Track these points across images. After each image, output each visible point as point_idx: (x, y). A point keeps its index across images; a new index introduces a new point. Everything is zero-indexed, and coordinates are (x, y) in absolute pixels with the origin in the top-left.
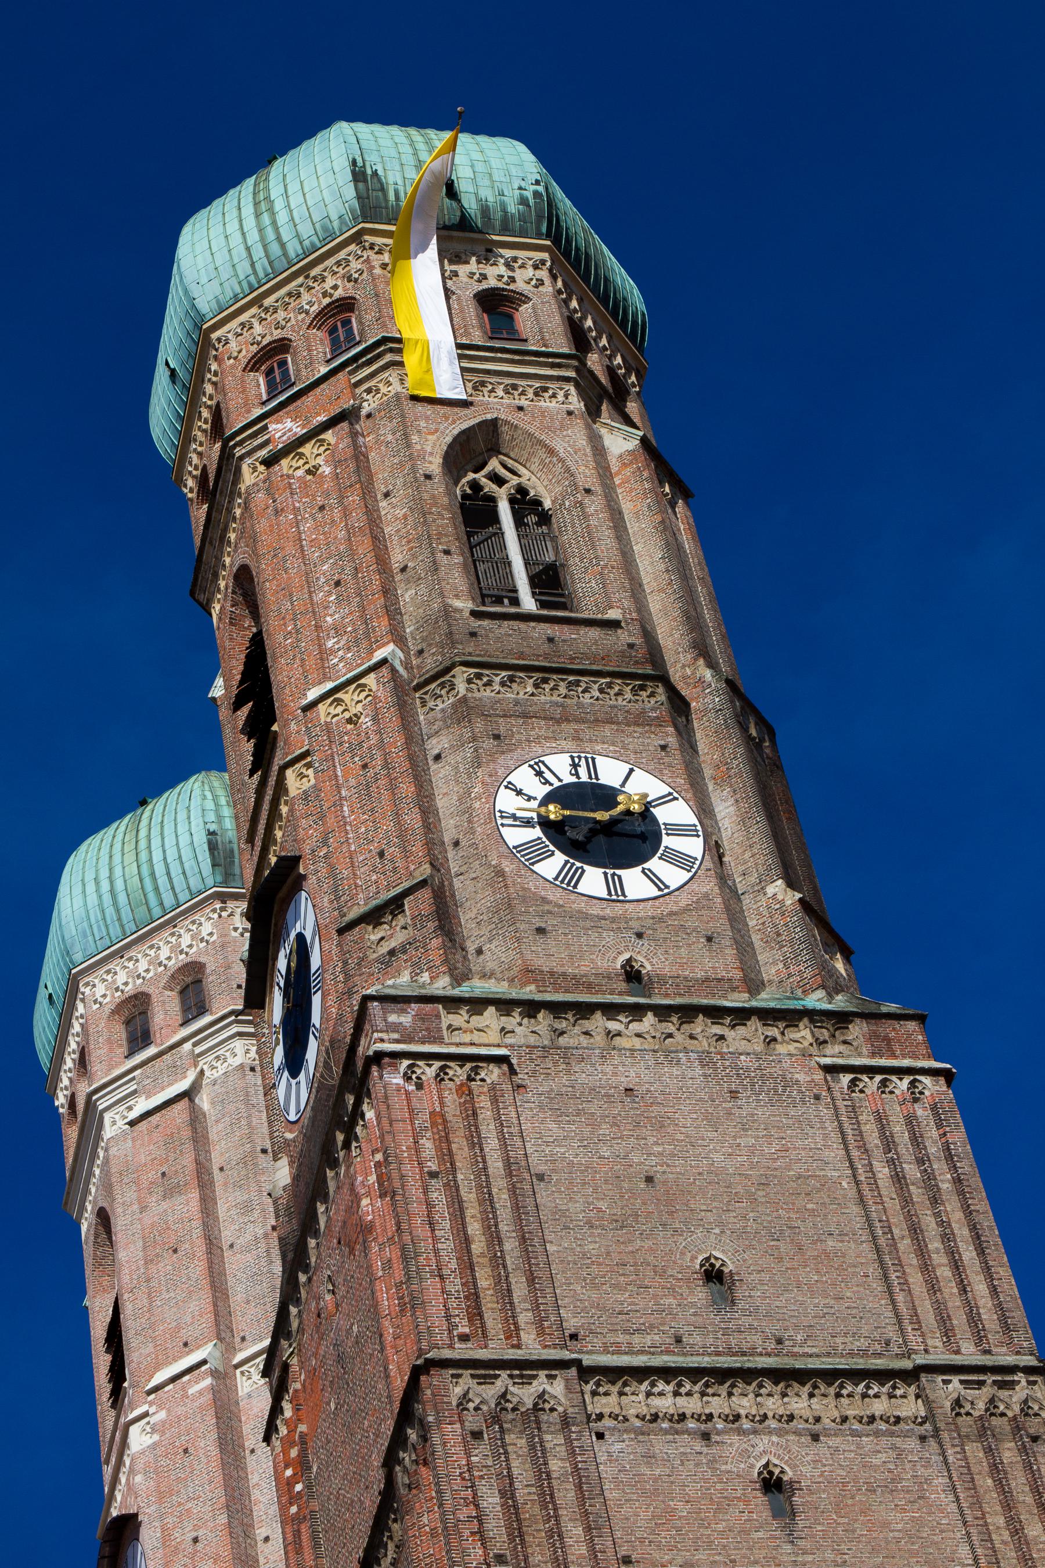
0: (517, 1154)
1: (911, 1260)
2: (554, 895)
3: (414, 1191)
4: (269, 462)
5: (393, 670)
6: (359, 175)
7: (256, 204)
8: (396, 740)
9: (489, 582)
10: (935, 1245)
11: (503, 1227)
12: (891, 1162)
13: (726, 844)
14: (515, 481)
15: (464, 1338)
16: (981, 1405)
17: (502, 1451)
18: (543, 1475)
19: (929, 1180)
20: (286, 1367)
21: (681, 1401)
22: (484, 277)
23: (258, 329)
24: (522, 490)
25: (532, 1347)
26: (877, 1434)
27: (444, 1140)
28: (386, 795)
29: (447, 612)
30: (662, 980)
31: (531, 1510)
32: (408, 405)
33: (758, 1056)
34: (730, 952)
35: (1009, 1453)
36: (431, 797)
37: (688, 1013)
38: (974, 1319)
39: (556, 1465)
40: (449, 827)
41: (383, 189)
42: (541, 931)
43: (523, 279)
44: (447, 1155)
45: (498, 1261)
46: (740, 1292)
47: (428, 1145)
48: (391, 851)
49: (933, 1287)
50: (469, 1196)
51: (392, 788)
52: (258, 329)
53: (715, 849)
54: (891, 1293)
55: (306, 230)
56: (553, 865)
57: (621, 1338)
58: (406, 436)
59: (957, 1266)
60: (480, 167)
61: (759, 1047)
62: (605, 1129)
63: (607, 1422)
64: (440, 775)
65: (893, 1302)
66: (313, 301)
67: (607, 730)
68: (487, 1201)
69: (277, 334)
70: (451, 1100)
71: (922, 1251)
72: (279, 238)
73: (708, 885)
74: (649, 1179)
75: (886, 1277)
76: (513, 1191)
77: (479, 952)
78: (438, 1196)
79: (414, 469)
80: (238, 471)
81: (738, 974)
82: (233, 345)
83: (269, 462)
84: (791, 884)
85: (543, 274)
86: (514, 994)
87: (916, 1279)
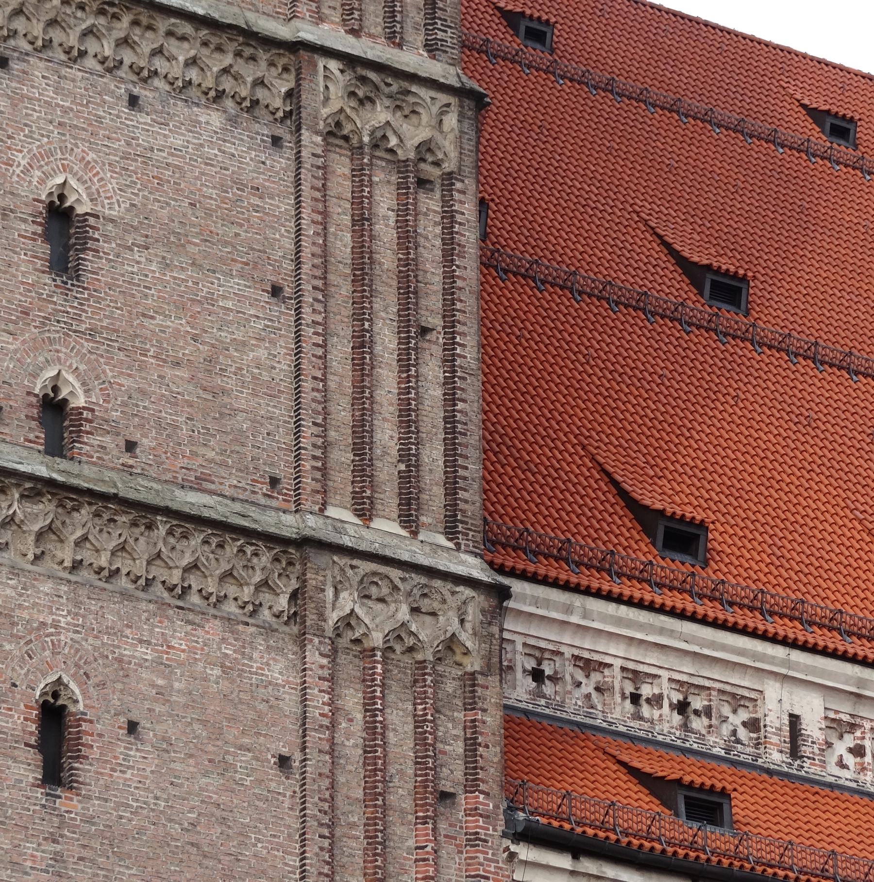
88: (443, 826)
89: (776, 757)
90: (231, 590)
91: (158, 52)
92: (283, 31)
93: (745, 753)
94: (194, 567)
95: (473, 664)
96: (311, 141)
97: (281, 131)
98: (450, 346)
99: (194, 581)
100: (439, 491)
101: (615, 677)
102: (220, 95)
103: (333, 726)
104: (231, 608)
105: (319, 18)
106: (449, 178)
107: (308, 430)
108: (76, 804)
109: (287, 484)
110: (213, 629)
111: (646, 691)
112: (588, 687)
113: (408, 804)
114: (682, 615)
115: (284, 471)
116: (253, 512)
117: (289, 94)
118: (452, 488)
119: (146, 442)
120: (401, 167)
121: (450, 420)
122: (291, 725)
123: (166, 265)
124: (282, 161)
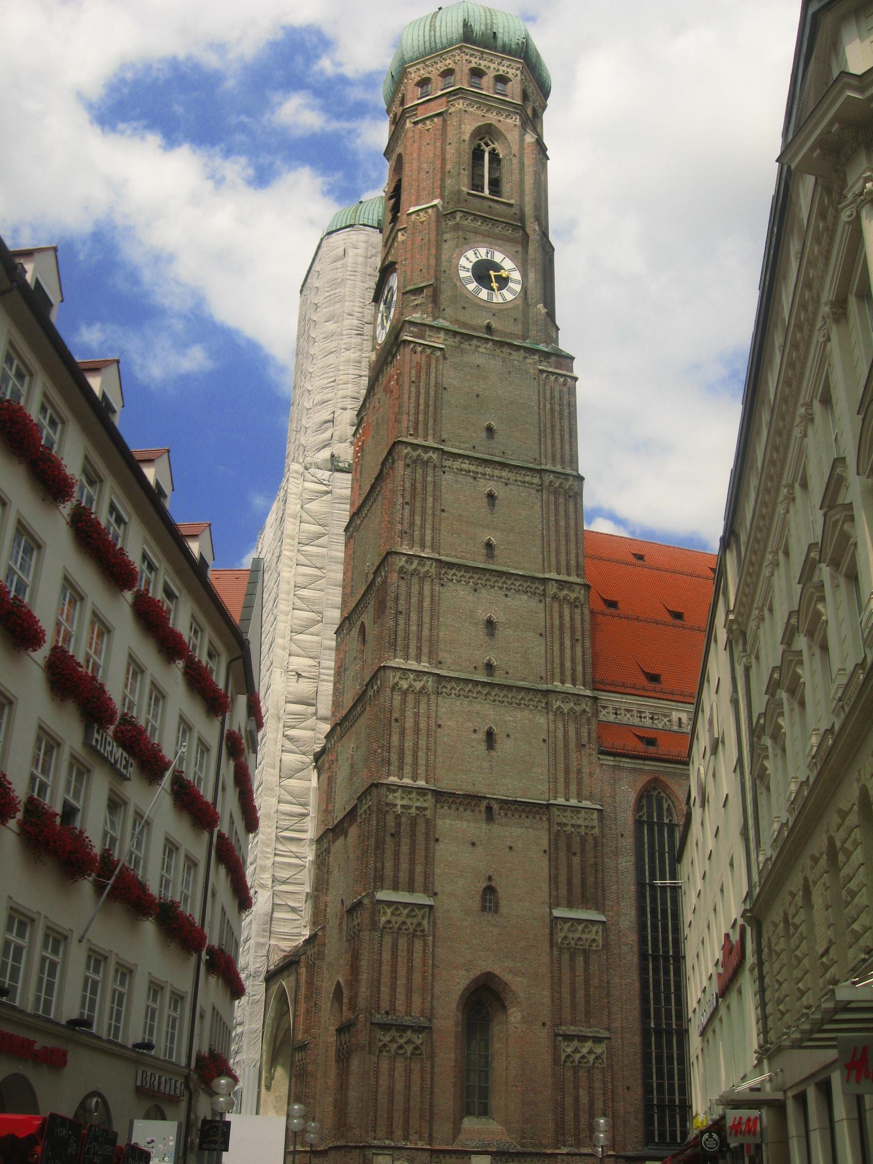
0: (439, 380)
1: (549, 435)
2: (469, 296)
3: (406, 386)
4: (416, 123)
5: (438, 209)
6: (466, 25)
7: (431, 26)
8: (433, 236)
9: (477, 182)
10: (557, 432)
11: (430, 403)
12: (551, 404)
13: (529, 286)
14: (492, 146)
15: (411, 435)
16: (557, 484)
17: (414, 472)
18: (425, 480)
19: (561, 412)
20: (362, 418)
21: (471, 466)
22: (498, 70)
23: (422, 72)
24: (494, 150)
25: (430, 443)
26: (525, 487)
27: (419, 372)
28: (426, 251)
29: (459, 191)
30: (497, 331)
31: (419, 490)
32: (463, 113)
33: (520, 362)
34: (520, 326)
35: (561, 500)
36: (440, 255)
37: (502, 344)
38: (562, 457)
39: (429, 479)
40: (444, 265)
41: (472, 32)
42: (464, 308)
43: (511, 73)
44: (418, 377)
45: (426, 413)
46: (496, 436)
47: (413, 372)
48: (424, 270)
49: (553, 445)
50: (422, 391)
51: (429, 250)
52: (422, 72)
53: (525, 290)
54: (540, 444)
55: (444, 41)
56: (472, 286)
57: (457, 443)
58: (460, 124)
59: (562, 440)
60: (506, 29)
61: (521, 359)
62: (468, 377)
63: (447, 469)
64: (446, 246)
65: (540, 448)
66: (441, 67)
67: (500, 242)
68: (427, 394)
69: (428, 75)
70: (424, 358)
71: (553, 433)
72: (435, 41)
73: (519, 302)
74: (478, 396)
75: (540, 440)
76: (436, 392)
77: (444, 310)
78: (413, 389)
79: (460, 137)
80: (405, 121)
81: (520, 333)
82: (413, 75)
83: (416, 123)
84: (545, 306)
85: (518, 72)
86: (450, 328)
87: (549, 442)
88: (583, 752)
89: (675, 728)
90: (531, 703)
91: (512, 584)
92: (541, 576)
93: (667, 728)
94: (522, 698)
95: (589, 715)
96: (548, 600)
97: (542, 598)
98: (583, 643)
99: (522, 702)
100: (581, 676)
101: (635, 713)
102: (527, 592)
103: (555, 732)
104: (531, 707)
105: (550, 571)
106: (582, 605)
107: (549, 665)
108: (495, 753)
109: (544, 678)
110: (526, 712)
111: (643, 715)
112: (628, 716)
113: (574, 748)
114: (650, 697)
115: (543, 675)
116: (536, 685)
117: (544, 590)
118: (584, 675)
119: (511, 671)
120: (570, 603)
121: (583, 660)
122: (546, 732)
123: (515, 631)
124: (542, 605)
